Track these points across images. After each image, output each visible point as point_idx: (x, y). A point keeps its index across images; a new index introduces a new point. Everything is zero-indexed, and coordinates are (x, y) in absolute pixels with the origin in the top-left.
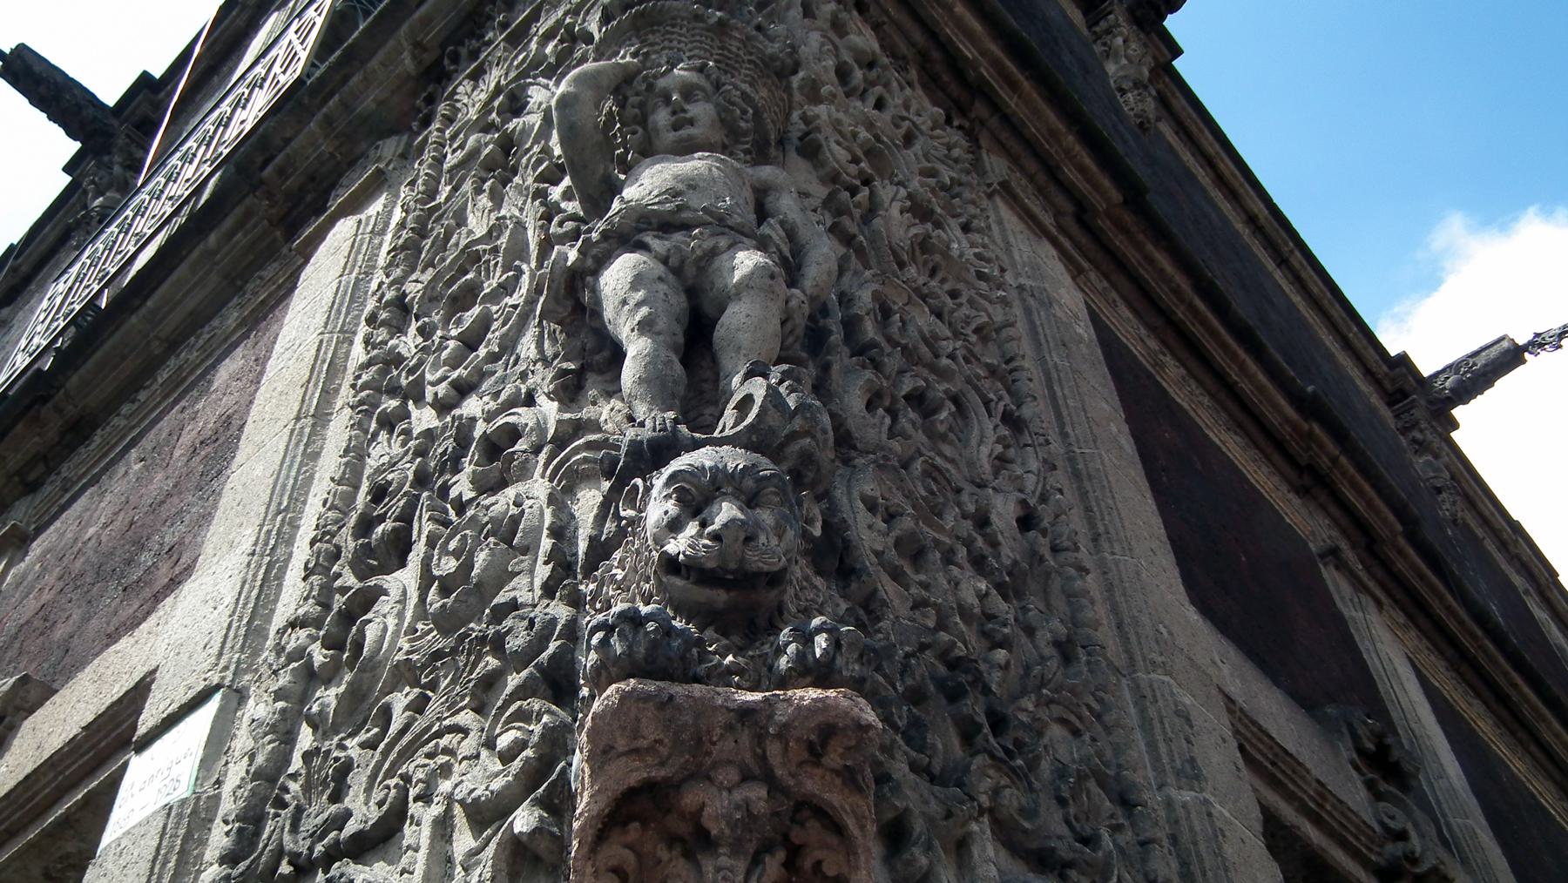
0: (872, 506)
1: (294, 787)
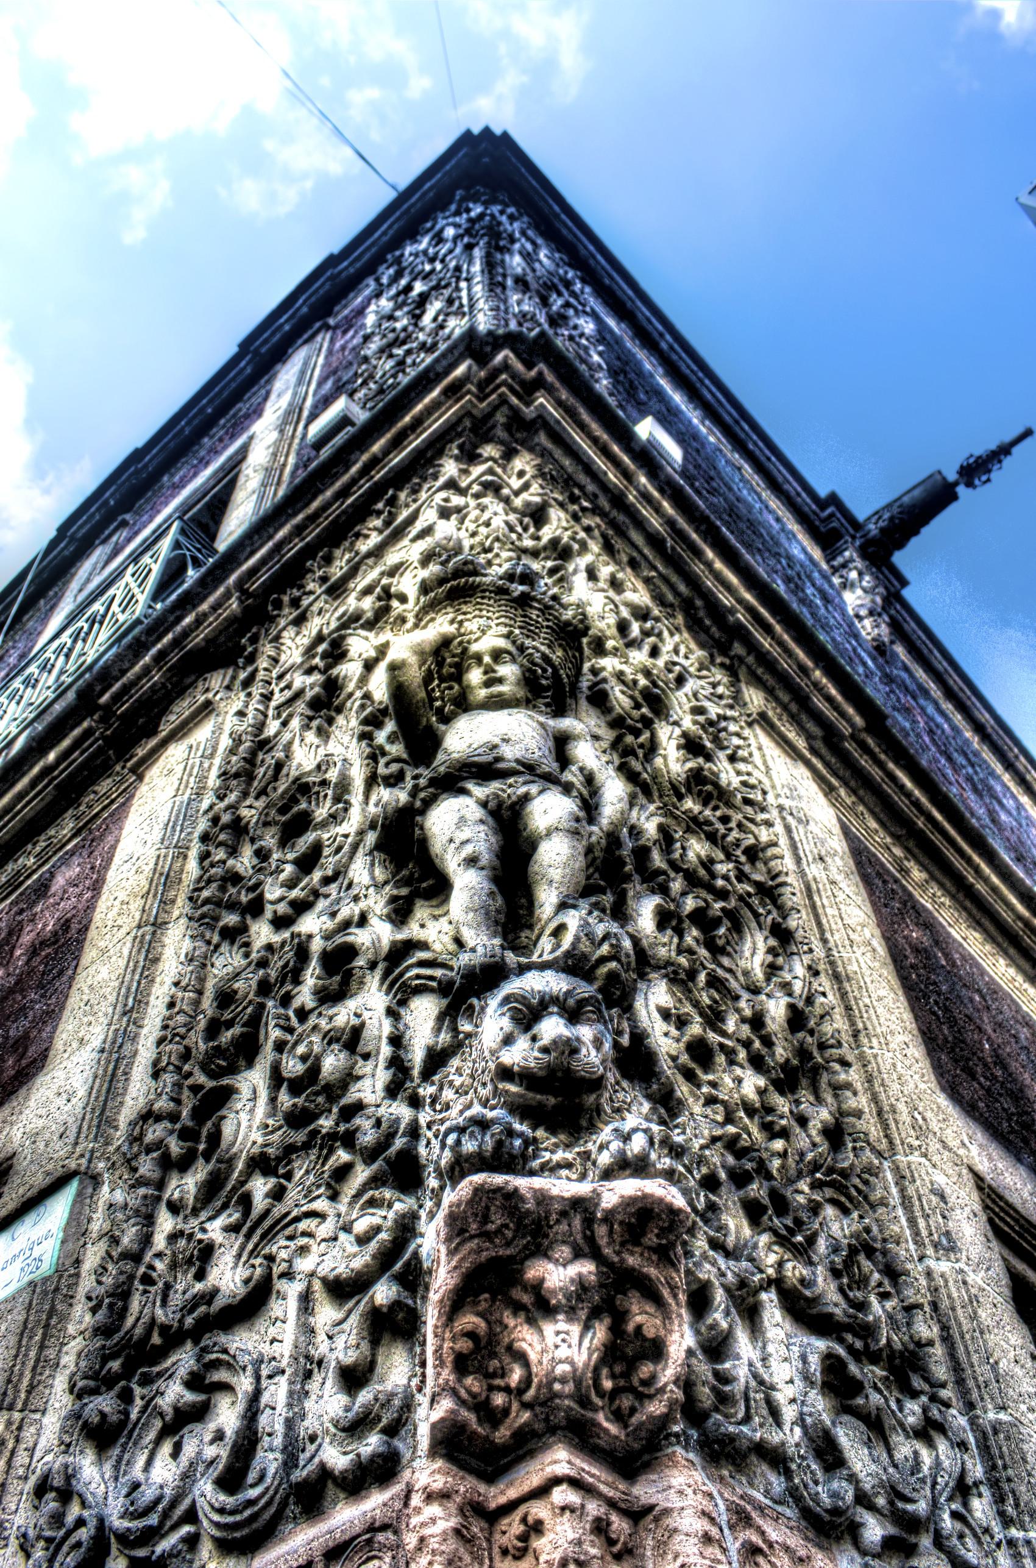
0: (665, 1014)
1: (160, 1265)
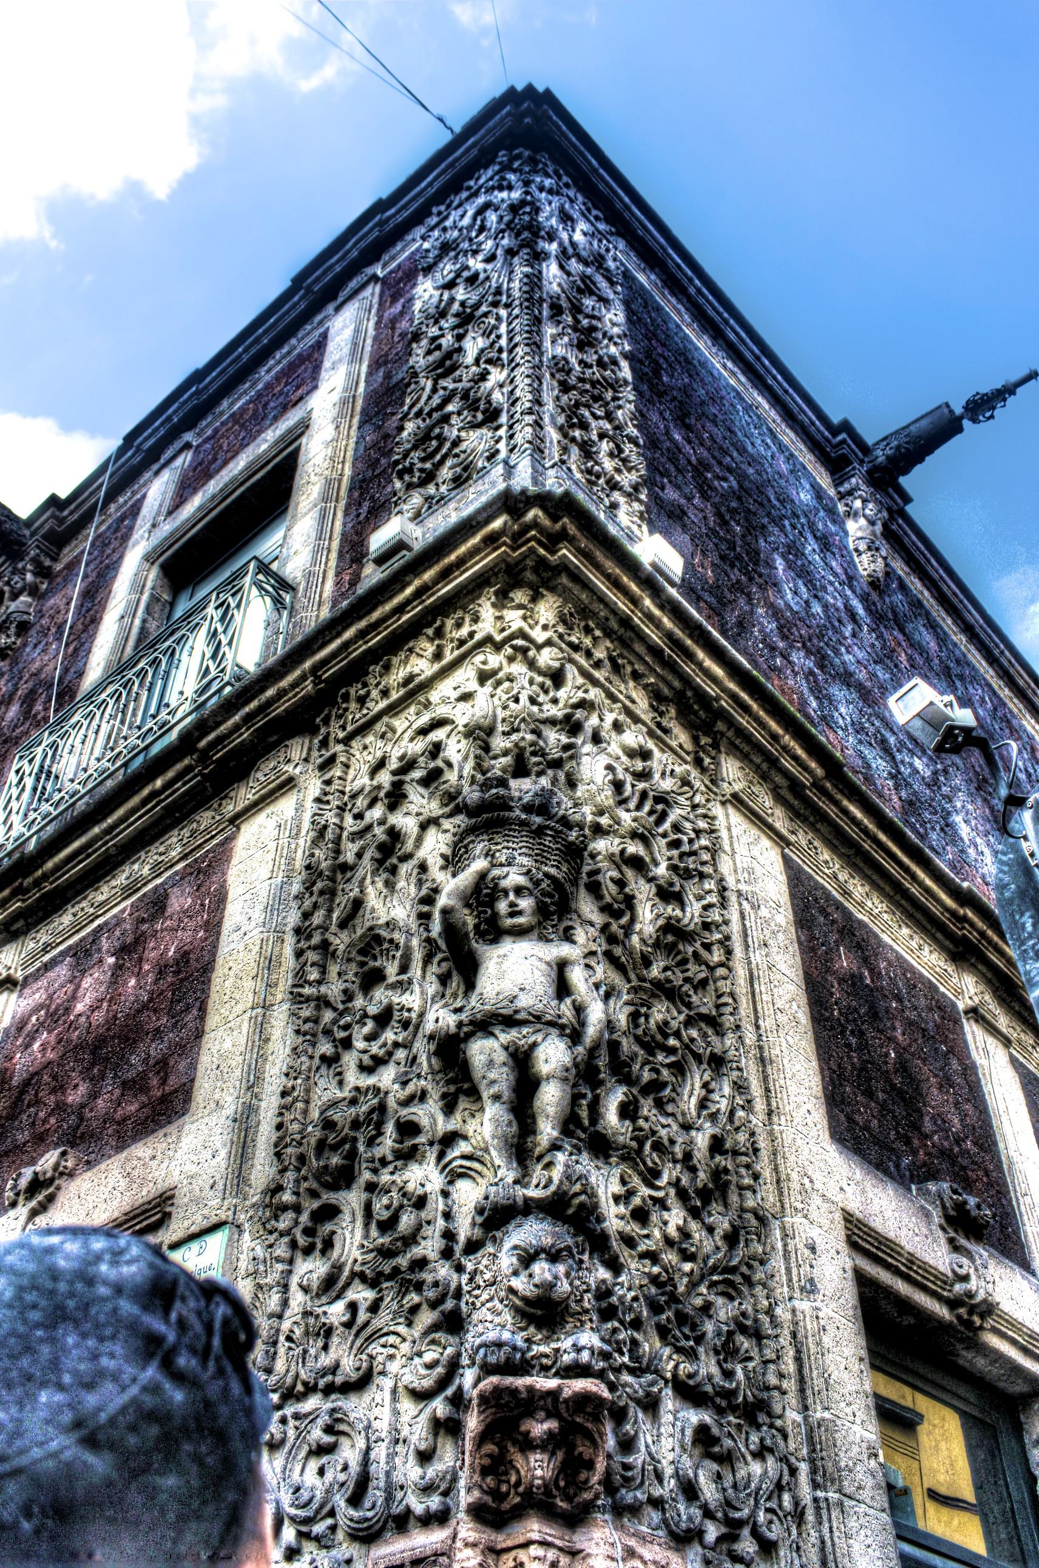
0: (617, 1199)
